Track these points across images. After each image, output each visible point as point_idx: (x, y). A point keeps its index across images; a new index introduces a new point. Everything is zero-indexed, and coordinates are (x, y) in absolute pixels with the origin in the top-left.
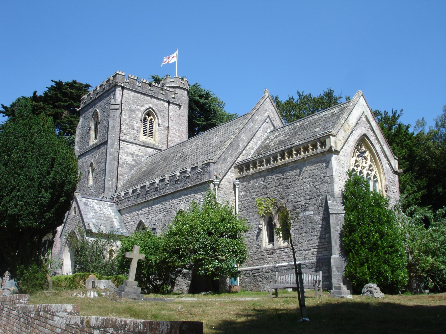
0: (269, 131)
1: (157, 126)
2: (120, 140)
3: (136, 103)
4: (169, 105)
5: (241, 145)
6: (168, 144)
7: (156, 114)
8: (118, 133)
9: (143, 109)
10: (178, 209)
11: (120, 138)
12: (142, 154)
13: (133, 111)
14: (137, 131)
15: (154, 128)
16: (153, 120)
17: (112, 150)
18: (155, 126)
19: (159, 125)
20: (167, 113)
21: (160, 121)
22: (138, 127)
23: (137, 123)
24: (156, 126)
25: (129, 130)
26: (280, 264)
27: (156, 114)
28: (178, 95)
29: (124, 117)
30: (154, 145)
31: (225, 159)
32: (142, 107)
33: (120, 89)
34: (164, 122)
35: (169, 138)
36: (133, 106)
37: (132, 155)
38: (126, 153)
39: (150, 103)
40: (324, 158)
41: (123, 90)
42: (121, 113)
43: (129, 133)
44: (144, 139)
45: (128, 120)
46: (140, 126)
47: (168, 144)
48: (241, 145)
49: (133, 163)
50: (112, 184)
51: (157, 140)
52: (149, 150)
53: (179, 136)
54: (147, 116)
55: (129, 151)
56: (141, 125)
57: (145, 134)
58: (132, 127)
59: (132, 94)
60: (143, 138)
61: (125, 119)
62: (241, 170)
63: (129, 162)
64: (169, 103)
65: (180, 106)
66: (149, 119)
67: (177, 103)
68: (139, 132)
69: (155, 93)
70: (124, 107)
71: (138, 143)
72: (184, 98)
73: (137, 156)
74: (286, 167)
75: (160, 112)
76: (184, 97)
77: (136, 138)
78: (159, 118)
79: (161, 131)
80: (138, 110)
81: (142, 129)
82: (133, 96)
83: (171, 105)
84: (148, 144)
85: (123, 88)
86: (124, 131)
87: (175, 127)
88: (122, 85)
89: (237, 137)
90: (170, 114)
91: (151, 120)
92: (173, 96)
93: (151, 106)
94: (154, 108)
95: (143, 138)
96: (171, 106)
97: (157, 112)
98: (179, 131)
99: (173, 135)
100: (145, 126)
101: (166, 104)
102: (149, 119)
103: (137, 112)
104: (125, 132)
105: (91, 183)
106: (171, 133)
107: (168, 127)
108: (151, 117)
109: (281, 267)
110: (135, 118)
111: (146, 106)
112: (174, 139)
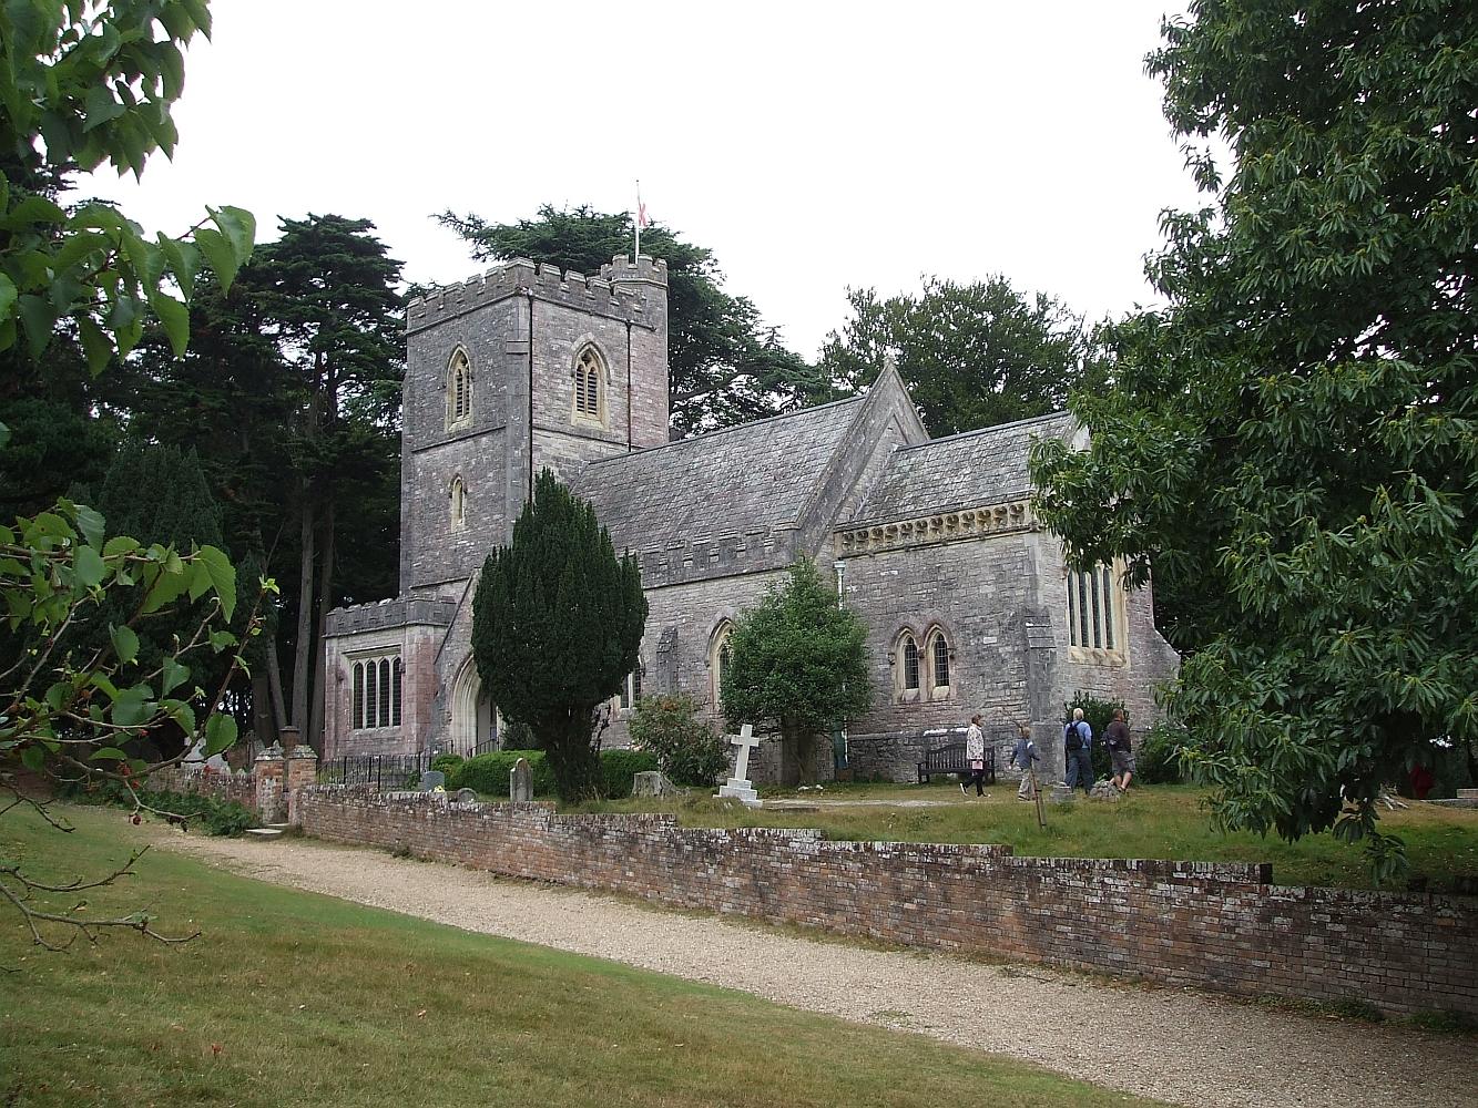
0: (896, 447)
1: (606, 386)
2: (531, 428)
3: (560, 335)
4: (629, 331)
6: (629, 426)
7: (603, 356)
8: (527, 414)
9: (577, 344)
10: (719, 616)
11: (531, 422)
12: (576, 457)
13: (554, 354)
15: (598, 385)
18: (602, 387)
21: (612, 372)
25: (548, 401)
26: (932, 732)
27: (603, 356)
29: (537, 370)
31: (818, 518)
33: (527, 302)
34: (619, 374)
36: (554, 341)
37: (554, 458)
38: (544, 457)
39: (589, 330)
40: (1020, 541)
41: (531, 305)
42: (531, 362)
44: (580, 421)
45: (546, 378)
46: (570, 389)
47: (629, 426)
51: (608, 418)
52: (593, 445)
53: (652, 406)
54: (583, 363)
57: (581, 407)
59: (550, 310)
60: (577, 418)
62: (850, 539)
64: (629, 326)
65: (652, 330)
66: (587, 369)
67: (644, 323)
69: (599, 304)
72: (658, 302)
73: (568, 461)
74: (945, 548)
75: (610, 349)
76: (662, 306)
77: (564, 419)
78: (610, 367)
79: (617, 398)
81: (576, 395)
84: (589, 432)
87: (643, 385)
89: (837, 470)
91: (592, 369)
92: (636, 306)
93: (591, 337)
96: (636, 333)
97: (603, 349)
98: (652, 393)
101: (623, 330)
102: (587, 369)
103: (564, 357)
104: (541, 408)
105: (458, 524)
107: (629, 386)
108: (593, 364)
109: (934, 736)
111: (582, 339)
112: (641, 413)
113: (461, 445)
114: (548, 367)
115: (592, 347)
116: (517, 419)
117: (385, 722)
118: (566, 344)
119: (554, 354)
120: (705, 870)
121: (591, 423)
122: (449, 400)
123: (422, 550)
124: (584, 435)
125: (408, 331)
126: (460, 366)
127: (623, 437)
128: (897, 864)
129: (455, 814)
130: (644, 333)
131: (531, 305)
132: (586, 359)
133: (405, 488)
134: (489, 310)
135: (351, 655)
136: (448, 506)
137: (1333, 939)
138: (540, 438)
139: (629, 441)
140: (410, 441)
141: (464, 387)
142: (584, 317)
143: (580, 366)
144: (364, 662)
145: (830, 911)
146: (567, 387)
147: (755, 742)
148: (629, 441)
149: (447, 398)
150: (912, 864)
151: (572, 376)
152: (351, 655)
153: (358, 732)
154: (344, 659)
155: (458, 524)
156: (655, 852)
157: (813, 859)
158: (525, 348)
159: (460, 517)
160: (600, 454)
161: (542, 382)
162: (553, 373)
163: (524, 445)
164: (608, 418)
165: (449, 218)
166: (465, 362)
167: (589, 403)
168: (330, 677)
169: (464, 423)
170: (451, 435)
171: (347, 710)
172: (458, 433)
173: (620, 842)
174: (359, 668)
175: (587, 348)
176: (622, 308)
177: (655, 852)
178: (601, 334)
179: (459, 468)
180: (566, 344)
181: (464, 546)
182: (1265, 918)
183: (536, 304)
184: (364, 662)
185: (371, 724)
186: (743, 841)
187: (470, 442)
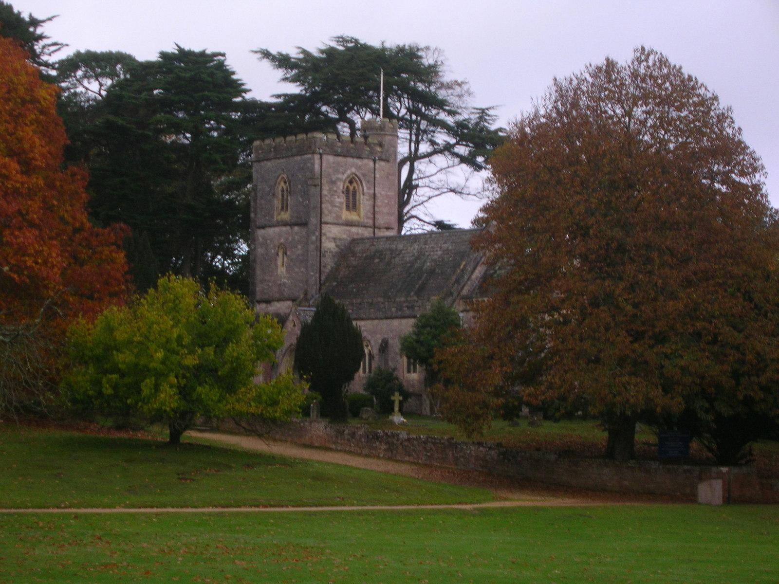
1: (362, 196)
2: (321, 223)
5: (466, 277)
9: (346, 175)
12: (345, 236)
13: (333, 182)
14: (338, 207)
16: (357, 188)
19: (363, 195)
20: (373, 175)
21: (365, 188)
22: (340, 203)
23: (338, 197)
24: (360, 196)
25: (330, 208)
27: (361, 182)
28: (386, 147)
29: (325, 192)
30: (358, 222)
32: (343, 174)
34: (369, 188)
35: (376, 209)
37: (334, 239)
38: (328, 238)
41: (321, 158)
43: (330, 212)
48: (466, 277)
49: (336, 249)
50: (316, 280)
52: (354, 230)
53: (388, 204)
54: (349, 185)
55: (331, 235)
57: (348, 208)
59: (331, 158)
60: (346, 215)
61: (326, 195)
63: (332, 250)
66: (351, 188)
68: (341, 209)
70: (324, 181)
71: (341, 222)
73: (340, 239)
75: (364, 175)
77: (338, 217)
78: (364, 185)
79: (367, 202)
80: (338, 179)
82: (333, 163)
83: (377, 162)
85: (321, 155)
86: (325, 212)
88: (321, 151)
90: (377, 176)
93: (353, 170)
94: (357, 173)
95: (346, 215)
97: (361, 178)
98: (387, 196)
99: (380, 204)
101: (371, 164)
102: (351, 188)
105: (281, 270)
106: (378, 202)
107: (374, 194)
108: (355, 184)
110: (336, 191)
111: (349, 172)
113: (284, 229)
114: (330, 190)
115: (354, 176)
116: (314, 220)
118: (340, 176)
119: (333, 182)
120: (376, 443)
121: (353, 217)
122: (277, 203)
123: (262, 281)
127: (371, 222)
128: (425, 443)
130: (383, 163)
131: (321, 158)
132: (351, 182)
134: (299, 158)
136: (276, 260)
138: (325, 228)
139: (374, 225)
141: (285, 196)
142: (350, 160)
143: (348, 188)
145: (409, 456)
146: (340, 199)
148: (374, 225)
150: (430, 442)
151: (343, 193)
155: (281, 270)
156: (361, 438)
157: (406, 440)
158: (318, 182)
159: (283, 266)
160: (358, 234)
161: (327, 198)
162: (333, 193)
163: (317, 234)
164: (362, 213)
166: (285, 182)
167: (352, 206)
169: (285, 216)
170: (278, 222)
173: (349, 434)
175: (351, 177)
176: (372, 152)
177: (361, 438)
178: (358, 168)
179: (282, 240)
180: (340, 176)
181: (284, 284)
182: (499, 456)
183: (325, 157)
186: (387, 434)
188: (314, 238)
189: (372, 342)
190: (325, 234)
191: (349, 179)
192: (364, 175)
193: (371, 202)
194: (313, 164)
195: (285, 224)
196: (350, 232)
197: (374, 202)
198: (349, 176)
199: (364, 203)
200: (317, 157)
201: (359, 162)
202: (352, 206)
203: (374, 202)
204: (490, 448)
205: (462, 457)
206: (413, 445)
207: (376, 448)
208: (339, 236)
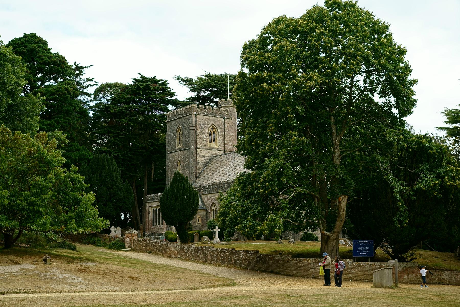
9: (209, 125)
12: (209, 155)
17: (193, 155)
21: (219, 132)
22: (206, 138)
29: (198, 133)
34: (221, 132)
35: (225, 142)
37: (204, 156)
38: (200, 156)
39: (213, 121)
49: (205, 161)
52: (214, 152)
56: (208, 137)
58: (202, 139)
60: (209, 144)
64: (224, 118)
67: (229, 117)
70: (197, 128)
73: (207, 156)
75: (219, 125)
80: (205, 127)
90: (226, 126)
93: (213, 123)
98: (231, 136)
100: (211, 137)
101: (223, 120)
102: (212, 132)
108: (214, 130)
111: (211, 124)
113: (180, 152)
117: (159, 224)
118: (206, 126)
121: (214, 145)
124: (211, 149)
125: (167, 121)
126: (179, 131)
127: (223, 148)
128: (221, 252)
129: (162, 245)
130: (229, 120)
132: (212, 129)
133: (167, 163)
135: (152, 207)
137: (262, 261)
138: (198, 151)
140: (168, 150)
143: (210, 131)
144: (155, 209)
147: (219, 230)
149: (177, 140)
152: (152, 207)
153: (153, 226)
154: (150, 208)
164: (218, 144)
165: (183, 80)
167: (213, 140)
168: (147, 212)
169: (180, 146)
171: (151, 222)
172: (179, 149)
174: (154, 210)
180: (206, 126)
182: (257, 259)
183: (197, 116)
184: (155, 209)
185: (156, 224)
186: (203, 248)
187: (182, 152)
188: (193, 155)
189: (217, 205)
190: (198, 154)
191: (211, 127)
192: (219, 125)
193: (223, 139)
194: (192, 120)
195: (180, 150)
196: (212, 153)
197: (224, 139)
198: (210, 126)
199: (219, 139)
200: (194, 116)
201: (216, 119)
202: (213, 140)
203: (224, 139)
204: (252, 254)
205: (238, 260)
206: (215, 254)
207: (198, 257)
208: (206, 155)
